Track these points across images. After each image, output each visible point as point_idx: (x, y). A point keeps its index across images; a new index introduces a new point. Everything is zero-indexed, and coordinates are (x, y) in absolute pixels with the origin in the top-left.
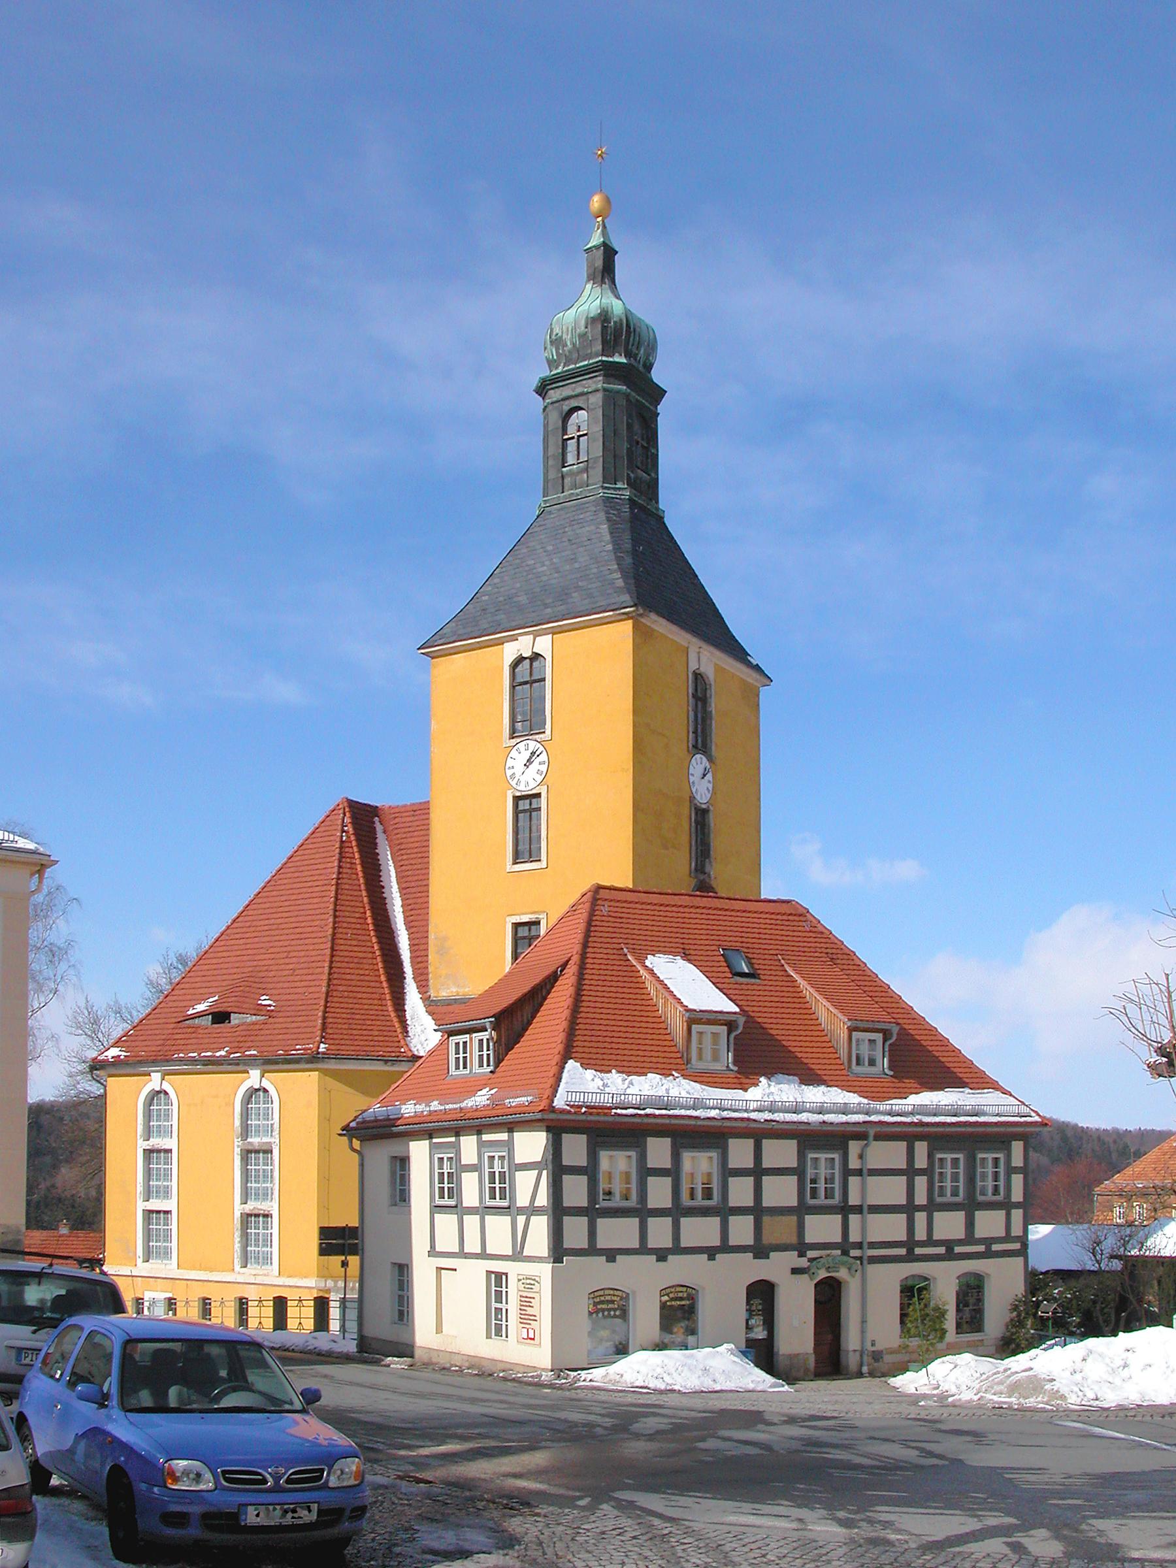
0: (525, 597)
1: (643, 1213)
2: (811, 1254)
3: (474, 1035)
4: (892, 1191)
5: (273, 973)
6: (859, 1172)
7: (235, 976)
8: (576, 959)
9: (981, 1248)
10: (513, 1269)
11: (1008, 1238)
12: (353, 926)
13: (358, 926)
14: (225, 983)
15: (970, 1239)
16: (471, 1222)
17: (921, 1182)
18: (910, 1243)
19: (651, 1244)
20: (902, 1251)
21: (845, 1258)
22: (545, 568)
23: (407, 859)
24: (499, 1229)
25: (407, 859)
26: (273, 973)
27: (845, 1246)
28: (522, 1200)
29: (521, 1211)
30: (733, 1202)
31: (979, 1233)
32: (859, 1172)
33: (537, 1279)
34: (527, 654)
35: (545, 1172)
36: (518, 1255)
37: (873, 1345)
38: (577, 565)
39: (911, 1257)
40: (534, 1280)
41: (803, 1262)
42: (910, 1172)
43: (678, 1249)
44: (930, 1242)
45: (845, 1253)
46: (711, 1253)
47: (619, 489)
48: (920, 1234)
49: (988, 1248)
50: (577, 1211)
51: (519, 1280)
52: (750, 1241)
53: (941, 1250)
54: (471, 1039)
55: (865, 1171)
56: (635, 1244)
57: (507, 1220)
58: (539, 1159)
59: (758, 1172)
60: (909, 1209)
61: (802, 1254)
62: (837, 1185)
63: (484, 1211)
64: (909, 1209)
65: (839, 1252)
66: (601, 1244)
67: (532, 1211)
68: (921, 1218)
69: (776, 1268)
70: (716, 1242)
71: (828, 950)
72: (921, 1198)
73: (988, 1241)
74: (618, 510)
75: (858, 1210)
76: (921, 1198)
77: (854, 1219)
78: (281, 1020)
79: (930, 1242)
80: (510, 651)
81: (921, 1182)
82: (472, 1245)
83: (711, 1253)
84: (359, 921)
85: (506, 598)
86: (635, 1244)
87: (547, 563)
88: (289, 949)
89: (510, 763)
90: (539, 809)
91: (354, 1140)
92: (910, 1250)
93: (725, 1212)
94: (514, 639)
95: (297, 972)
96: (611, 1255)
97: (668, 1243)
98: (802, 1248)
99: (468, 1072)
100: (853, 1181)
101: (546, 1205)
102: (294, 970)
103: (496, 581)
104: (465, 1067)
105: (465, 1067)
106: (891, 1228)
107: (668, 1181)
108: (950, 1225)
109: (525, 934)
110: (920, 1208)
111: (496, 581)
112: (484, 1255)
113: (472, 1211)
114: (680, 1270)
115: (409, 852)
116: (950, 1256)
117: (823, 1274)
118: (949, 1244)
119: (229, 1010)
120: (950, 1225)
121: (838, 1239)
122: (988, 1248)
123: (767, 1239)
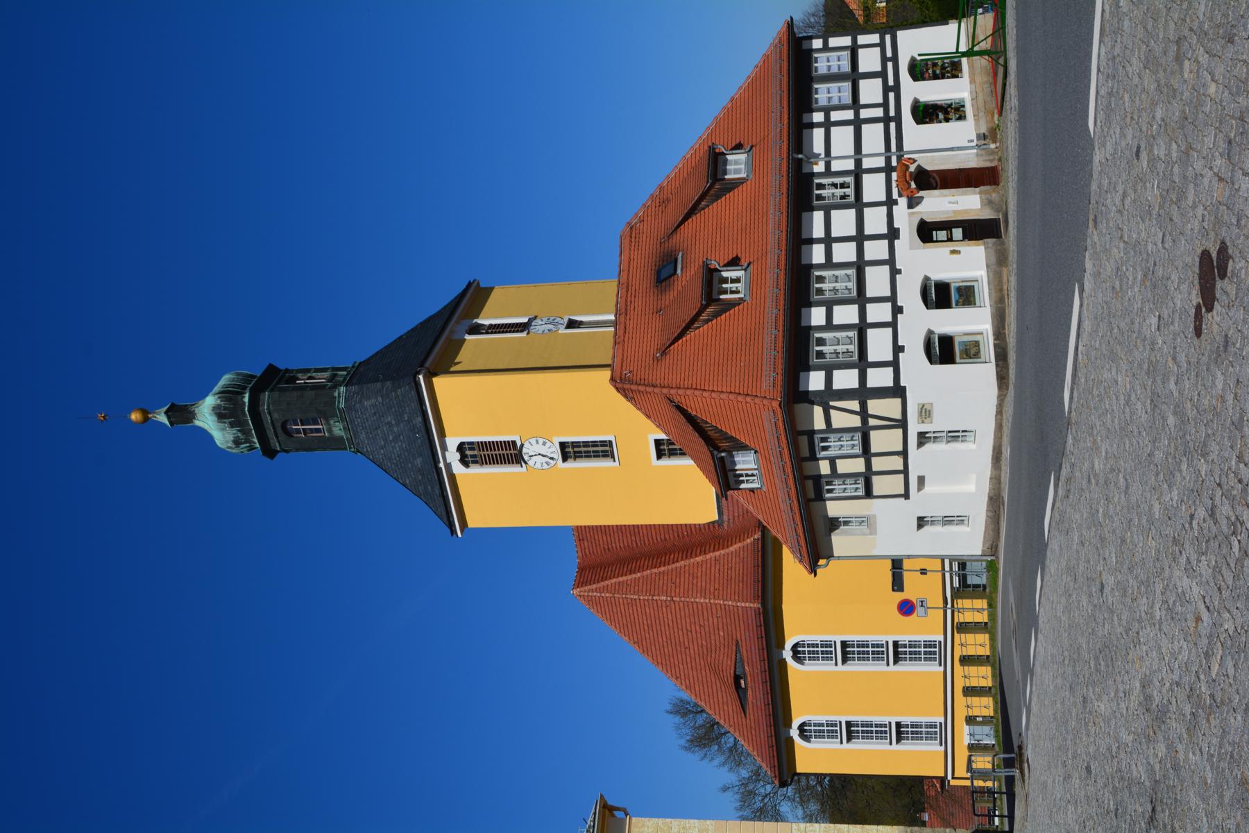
0: (418, 460)
1: (862, 328)
2: (895, 196)
3: (728, 468)
4: (842, 139)
5: (704, 643)
6: (828, 165)
7: (708, 671)
8: (665, 391)
9: (890, 65)
10: (914, 428)
11: (882, 45)
12: (665, 582)
13: (666, 578)
14: (713, 680)
15: (883, 74)
16: (877, 464)
17: (835, 116)
18: (886, 120)
20: (893, 125)
21: (898, 169)
22: (397, 445)
23: (615, 543)
24: (882, 440)
25: (615, 543)
26: (704, 643)
27: (888, 169)
28: (856, 421)
29: (864, 422)
30: (853, 258)
31: (877, 67)
32: (828, 165)
33: (921, 406)
34: (458, 456)
35: (832, 403)
36: (902, 424)
37: (972, 141)
38: (393, 422)
39: (898, 119)
40: (922, 409)
41: (903, 202)
42: (828, 125)
43: (893, 298)
44: (885, 105)
45: (892, 169)
46: (895, 272)
47: (339, 394)
48: (879, 112)
49: (890, 59)
50: (863, 378)
51: (923, 422)
52: (886, 242)
53: (891, 95)
56: (890, 330)
57: (873, 434)
58: (821, 408)
59: (828, 240)
60: (857, 124)
61: (896, 202)
62: (838, 180)
63: (866, 452)
64: (857, 124)
65: (894, 175)
66: (890, 358)
67: (864, 413)
68: (864, 114)
69: (905, 218)
70: (886, 268)
71: (658, 204)
72: (849, 115)
73: (884, 60)
75: (858, 163)
76: (849, 115)
77: (867, 163)
78: (738, 635)
79: (885, 105)
80: (458, 468)
81: (835, 116)
82: (897, 463)
83: (895, 272)
84: (661, 578)
86: (890, 330)
87: (393, 444)
88: (685, 631)
89: (538, 466)
90: (572, 443)
91: (819, 564)
92: (890, 120)
93: (860, 266)
94: (448, 466)
95: (702, 624)
96: (898, 349)
97: (888, 305)
98: (890, 203)
99: (757, 471)
100: (836, 166)
102: (700, 626)
103: (408, 482)
104: (753, 475)
105: (753, 475)
106: (873, 136)
107: (836, 309)
108: (871, 91)
109: (662, 449)
110: (857, 114)
111: (408, 482)
112: (904, 453)
113: (868, 465)
114: (909, 296)
115: (610, 542)
116: (896, 88)
117: (913, 185)
118: (886, 89)
119: (732, 675)
120: (871, 91)
121: (882, 176)
122: (890, 59)
123: (884, 230)
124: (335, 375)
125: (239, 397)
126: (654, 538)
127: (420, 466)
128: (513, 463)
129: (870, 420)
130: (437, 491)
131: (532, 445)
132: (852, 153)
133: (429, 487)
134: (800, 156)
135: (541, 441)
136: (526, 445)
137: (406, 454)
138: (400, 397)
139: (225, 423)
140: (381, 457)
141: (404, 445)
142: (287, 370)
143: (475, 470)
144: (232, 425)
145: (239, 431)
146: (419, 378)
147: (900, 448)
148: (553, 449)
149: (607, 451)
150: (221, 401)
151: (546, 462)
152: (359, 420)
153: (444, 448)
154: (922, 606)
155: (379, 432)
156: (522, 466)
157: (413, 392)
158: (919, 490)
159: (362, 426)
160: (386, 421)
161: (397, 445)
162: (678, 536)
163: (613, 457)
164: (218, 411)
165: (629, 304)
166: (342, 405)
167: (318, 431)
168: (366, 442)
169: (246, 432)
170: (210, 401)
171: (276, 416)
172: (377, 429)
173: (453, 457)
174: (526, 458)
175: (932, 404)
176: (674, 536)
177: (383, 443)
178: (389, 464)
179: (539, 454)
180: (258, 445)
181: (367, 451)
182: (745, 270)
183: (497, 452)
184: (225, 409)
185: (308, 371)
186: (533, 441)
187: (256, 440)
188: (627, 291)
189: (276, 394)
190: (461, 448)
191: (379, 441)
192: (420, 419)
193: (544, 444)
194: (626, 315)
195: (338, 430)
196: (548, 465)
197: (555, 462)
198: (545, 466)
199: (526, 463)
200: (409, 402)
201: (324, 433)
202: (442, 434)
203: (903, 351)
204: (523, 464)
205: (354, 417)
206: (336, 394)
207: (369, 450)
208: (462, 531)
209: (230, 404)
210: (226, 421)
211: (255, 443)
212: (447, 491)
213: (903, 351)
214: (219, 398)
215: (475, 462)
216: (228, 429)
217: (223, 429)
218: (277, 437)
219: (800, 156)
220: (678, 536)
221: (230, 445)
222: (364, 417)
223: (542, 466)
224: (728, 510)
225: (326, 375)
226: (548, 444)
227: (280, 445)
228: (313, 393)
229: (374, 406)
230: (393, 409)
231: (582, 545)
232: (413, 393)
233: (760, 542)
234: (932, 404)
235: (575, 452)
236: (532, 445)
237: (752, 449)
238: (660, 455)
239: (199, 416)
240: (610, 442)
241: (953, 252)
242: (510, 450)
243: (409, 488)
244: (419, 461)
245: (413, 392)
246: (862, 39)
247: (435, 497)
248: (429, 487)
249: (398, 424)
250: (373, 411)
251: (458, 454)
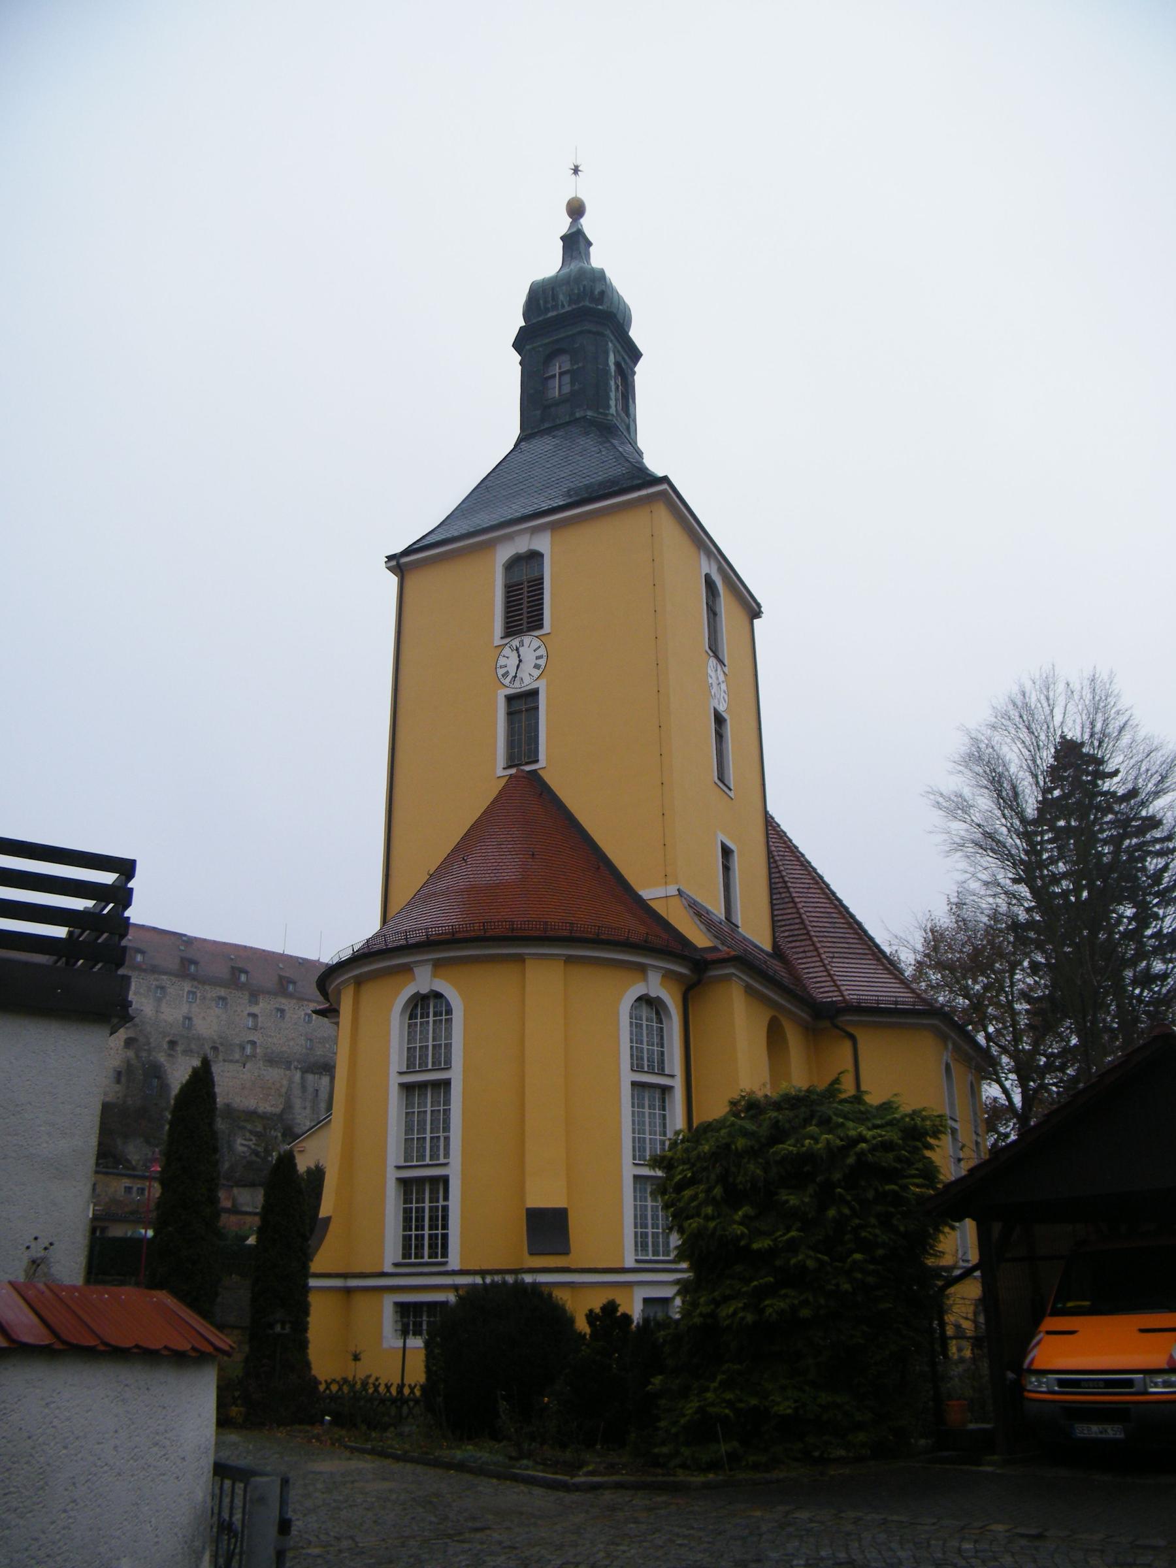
89: (502, 661)
131: (535, 651)
135: (542, 662)
148: (527, 680)
151: (508, 672)
153: (535, 530)
173: (521, 545)
179: (520, 661)
183: (525, 610)
186: (542, 651)
190: (535, 557)
193: (537, 667)
196: (503, 676)
202: (554, 527)
203: (591, 1311)
213: (591, 1311)
223: (501, 667)
226: (536, 673)
236: (535, 651)
240: (537, 761)
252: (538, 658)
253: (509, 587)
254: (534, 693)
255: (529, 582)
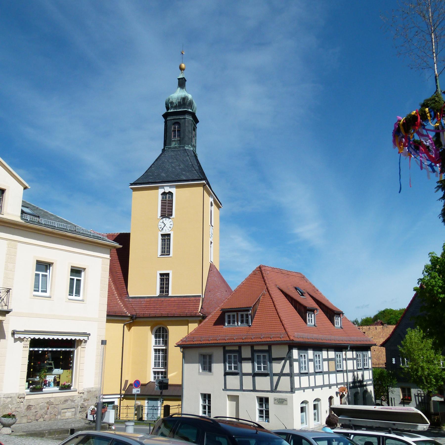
2: (339, 386)
11: (370, 380)
19: (311, 386)
34: (167, 191)
36: (274, 390)
41: (337, 390)
47: (190, 147)
54: (237, 315)
55: (347, 359)
65: (343, 386)
67: (281, 374)
70: (322, 384)
74: (190, 153)
80: (161, 191)
81: (355, 361)
83: (321, 387)
85: (158, 174)
87: (170, 165)
90: (170, 239)
94: (163, 187)
101: (289, 373)
103: (153, 169)
111: (153, 169)
112: (254, 390)
124: (194, 146)
125: (190, 108)
126: (117, 268)
127: (161, 175)
128: (161, 213)
129: (277, 377)
130: (150, 181)
131: (170, 222)
132: (348, 369)
133: (152, 177)
134: (349, 348)
136: (170, 220)
137: (166, 170)
138: (193, 172)
139: (181, 100)
140: (163, 159)
141: (170, 170)
142: (196, 128)
143: (160, 198)
144: (179, 103)
145: (177, 105)
146: (203, 181)
147: (257, 389)
149: (164, 252)
150: (190, 100)
152: (180, 153)
153: (171, 187)
154: (137, 391)
155: (175, 161)
156: (160, 217)
157: (196, 177)
158: (228, 396)
159: (177, 154)
160: (181, 164)
161: (170, 167)
162: (119, 279)
163: (162, 255)
164: (186, 98)
165: (284, 275)
166: (186, 148)
167: (175, 136)
168: (170, 155)
169: (176, 107)
170: (190, 96)
171: (183, 120)
172: (177, 160)
173: (167, 190)
174: (164, 219)
175: (287, 404)
176: (119, 277)
177: (170, 161)
178: (160, 162)
180: (169, 111)
181: (165, 154)
182: (314, 325)
184: (187, 101)
185: (196, 137)
186: (172, 223)
187: (172, 111)
188: (287, 274)
189: (191, 122)
190: (170, 193)
191: (171, 160)
192: (184, 178)
194: (281, 273)
195: (173, 145)
197: (161, 230)
198: (159, 227)
199: (161, 219)
200: (191, 175)
201: (173, 138)
202: (177, 187)
204: (161, 218)
205: (181, 152)
206: (190, 146)
207: (166, 155)
208: (130, 188)
209: (188, 103)
210: (182, 100)
211: (170, 110)
212: (151, 184)
214: (191, 100)
215: (163, 198)
216: (178, 100)
217: (178, 98)
218: (173, 119)
219: (349, 348)
220: (119, 279)
221: (171, 100)
222: (181, 156)
223: (160, 225)
224: (139, 301)
225: (194, 144)
226: (170, 229)
227: (169, 120)
228: (191, 137)
229: (187, 160)
230: (187, 168)
231: (111, 236)
232: (196, 178)
233: (125, 315)
234: (287, 404)
235: (165, 239)
236: (170, 222)
237: (251, 324)
238: (161, 275)
239: (182, 90)
240: (169, 255)
241: (327, 412)
242: (168, 213)
243: (150, 169)
244: (163, 175)
245: (196, 177)
246: (371, 371)
247: (147, 179)
248: (152, 177)
249: (180, 169)
250: (185, 160)
251: (168, 192)
252: (171, 225)
253: (162, 201)
254: (169, 235)
255: (168, 201)
